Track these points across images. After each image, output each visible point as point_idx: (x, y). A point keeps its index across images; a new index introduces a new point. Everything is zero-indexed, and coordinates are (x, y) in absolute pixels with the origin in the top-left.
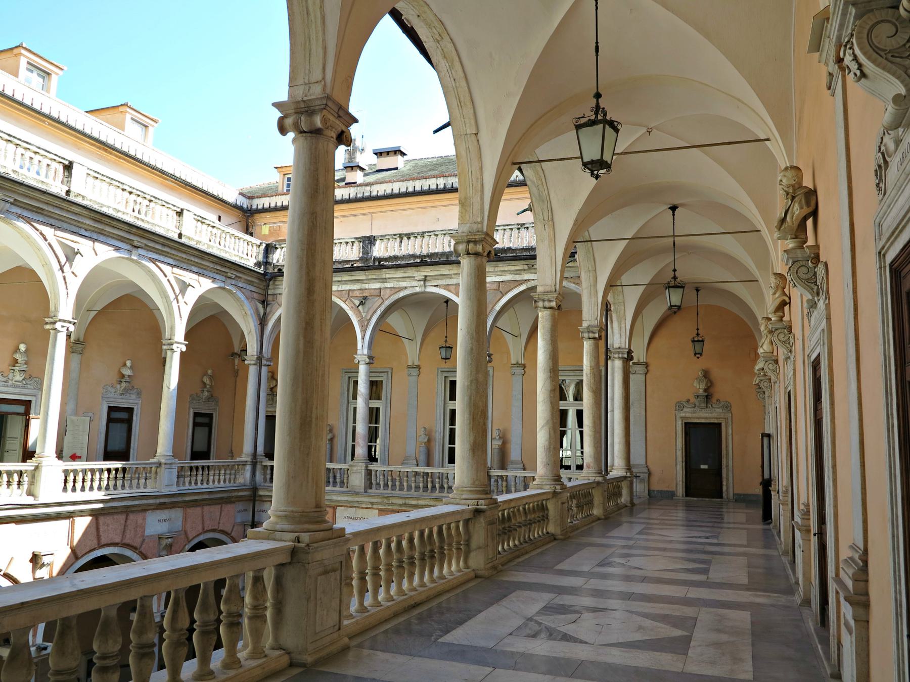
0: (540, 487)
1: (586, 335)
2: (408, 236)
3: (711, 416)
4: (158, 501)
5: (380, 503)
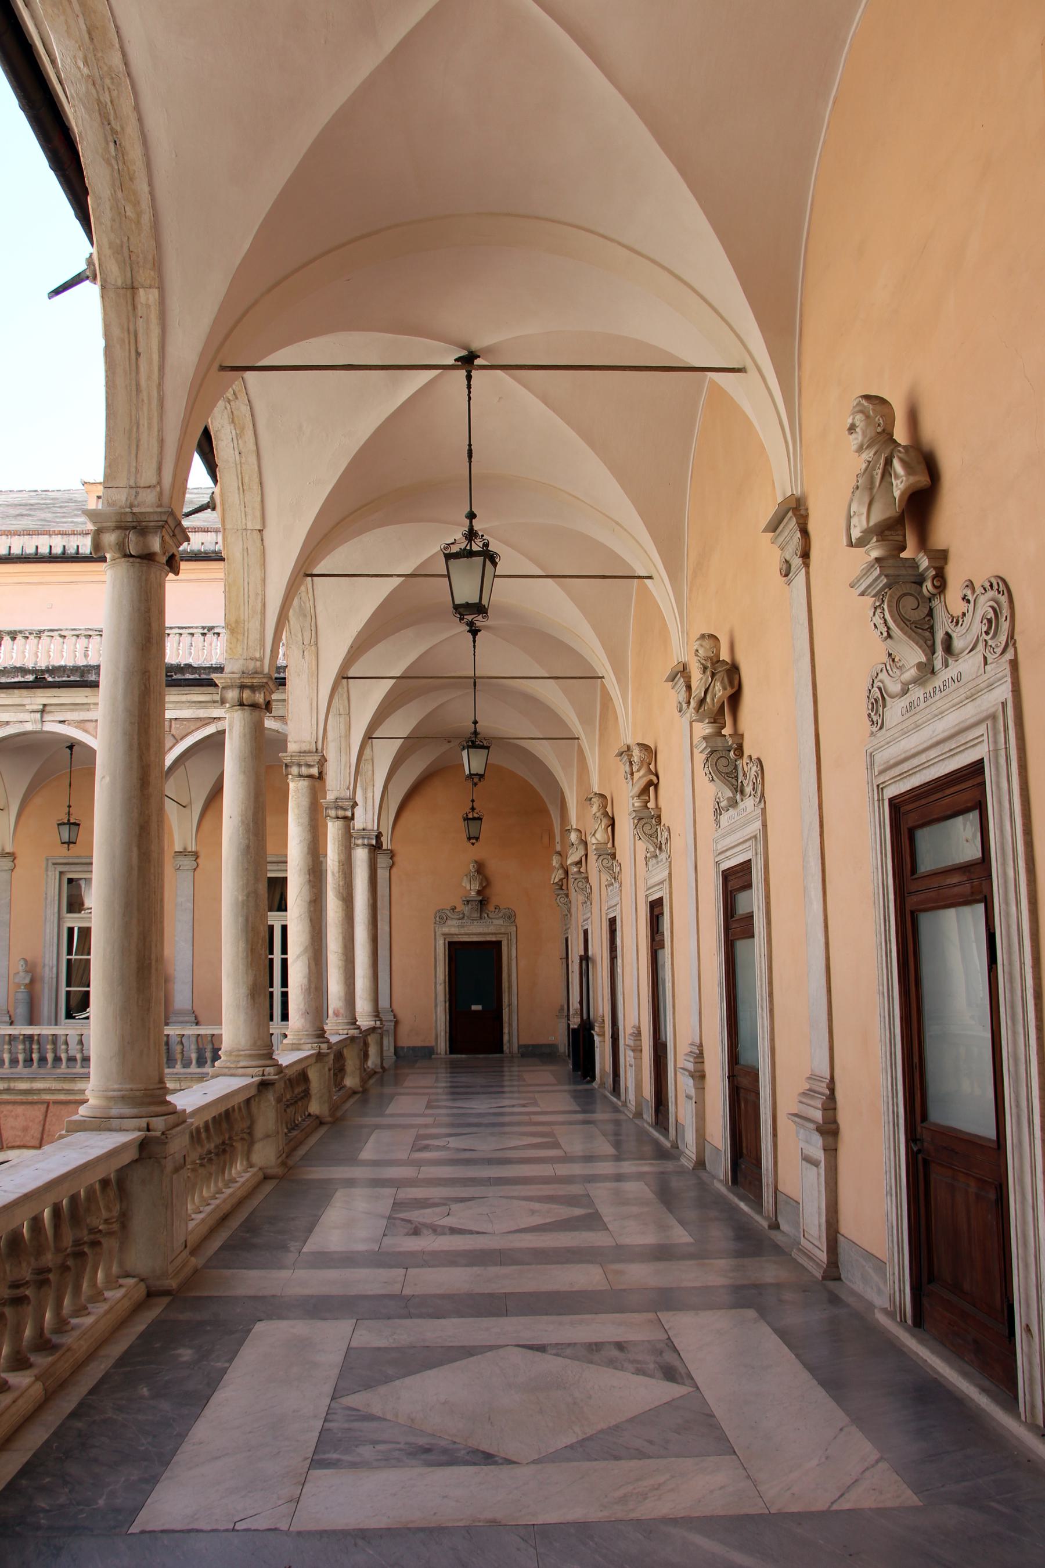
0: (295, 1047)
1: (332, 813)
3: (486, 930)
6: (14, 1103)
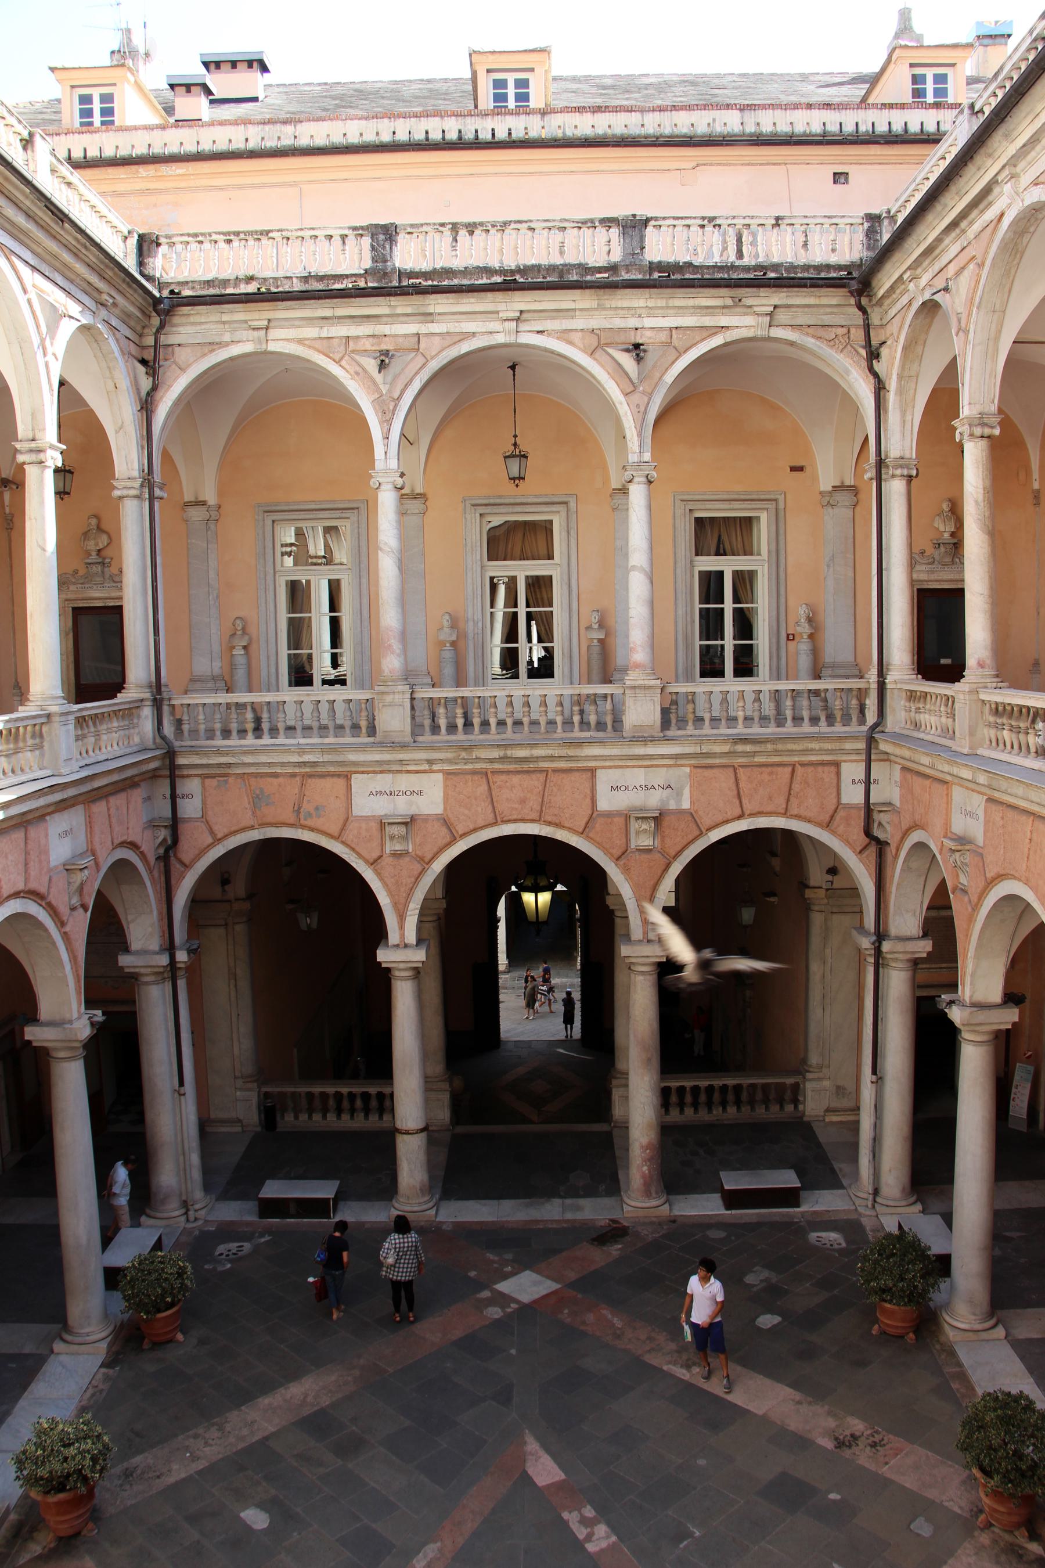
2: (471, 228)
4: (58, 797)
5: (449, 761)
6: (508, 772)
